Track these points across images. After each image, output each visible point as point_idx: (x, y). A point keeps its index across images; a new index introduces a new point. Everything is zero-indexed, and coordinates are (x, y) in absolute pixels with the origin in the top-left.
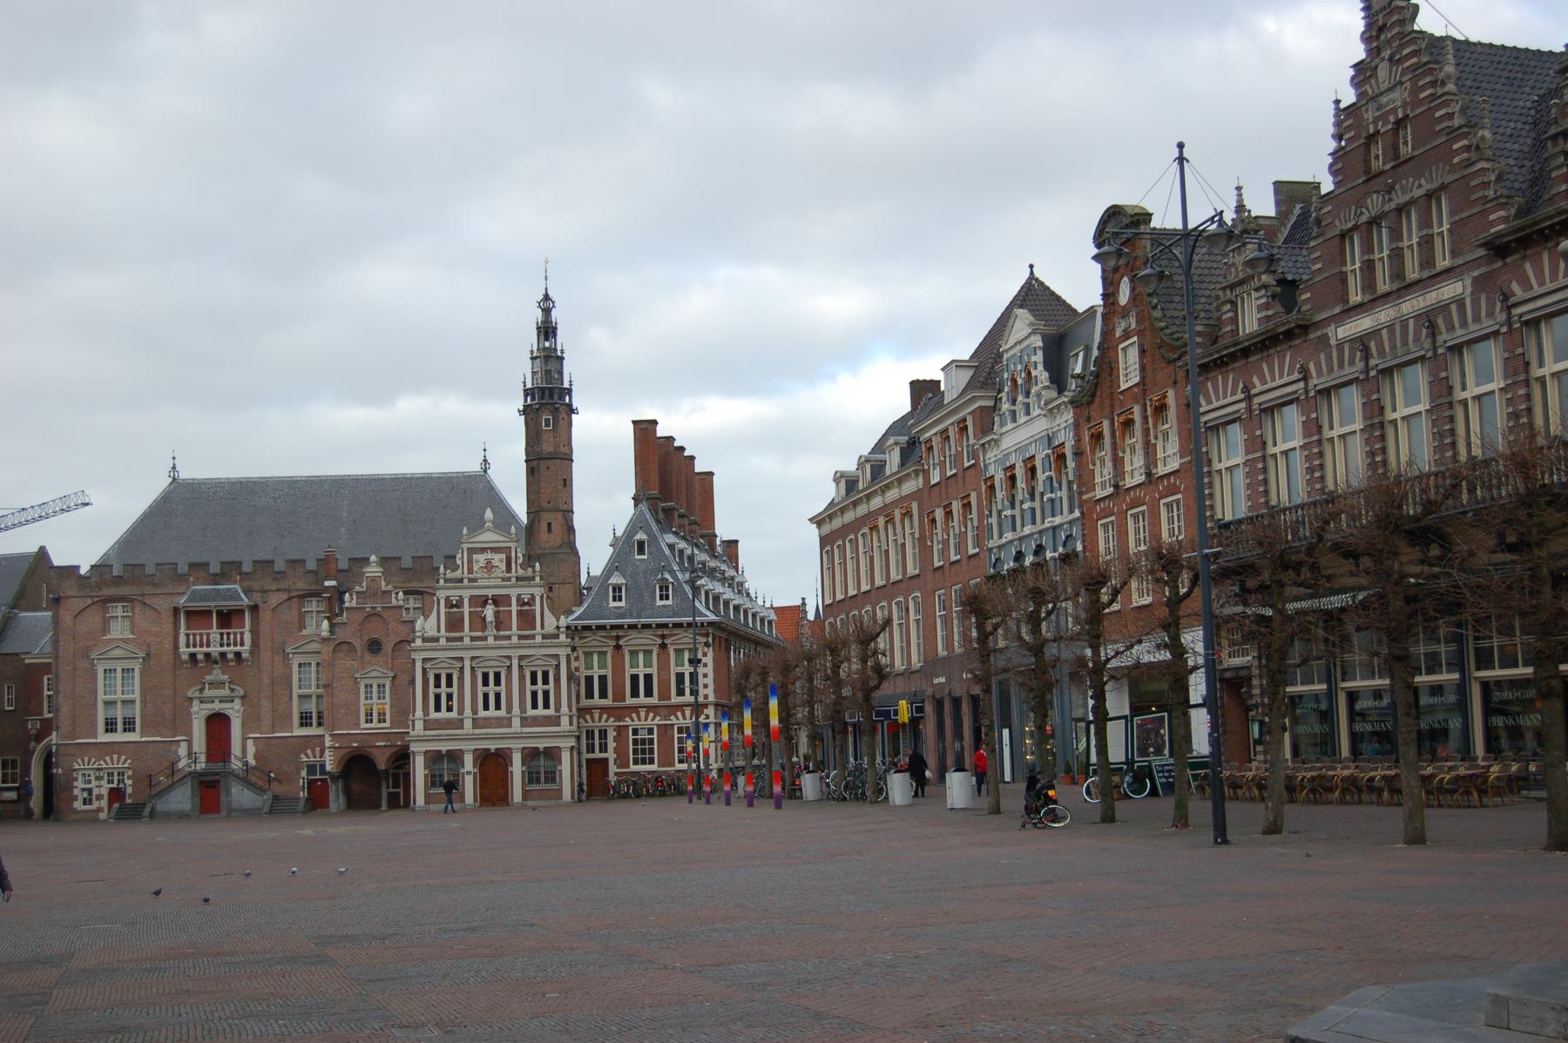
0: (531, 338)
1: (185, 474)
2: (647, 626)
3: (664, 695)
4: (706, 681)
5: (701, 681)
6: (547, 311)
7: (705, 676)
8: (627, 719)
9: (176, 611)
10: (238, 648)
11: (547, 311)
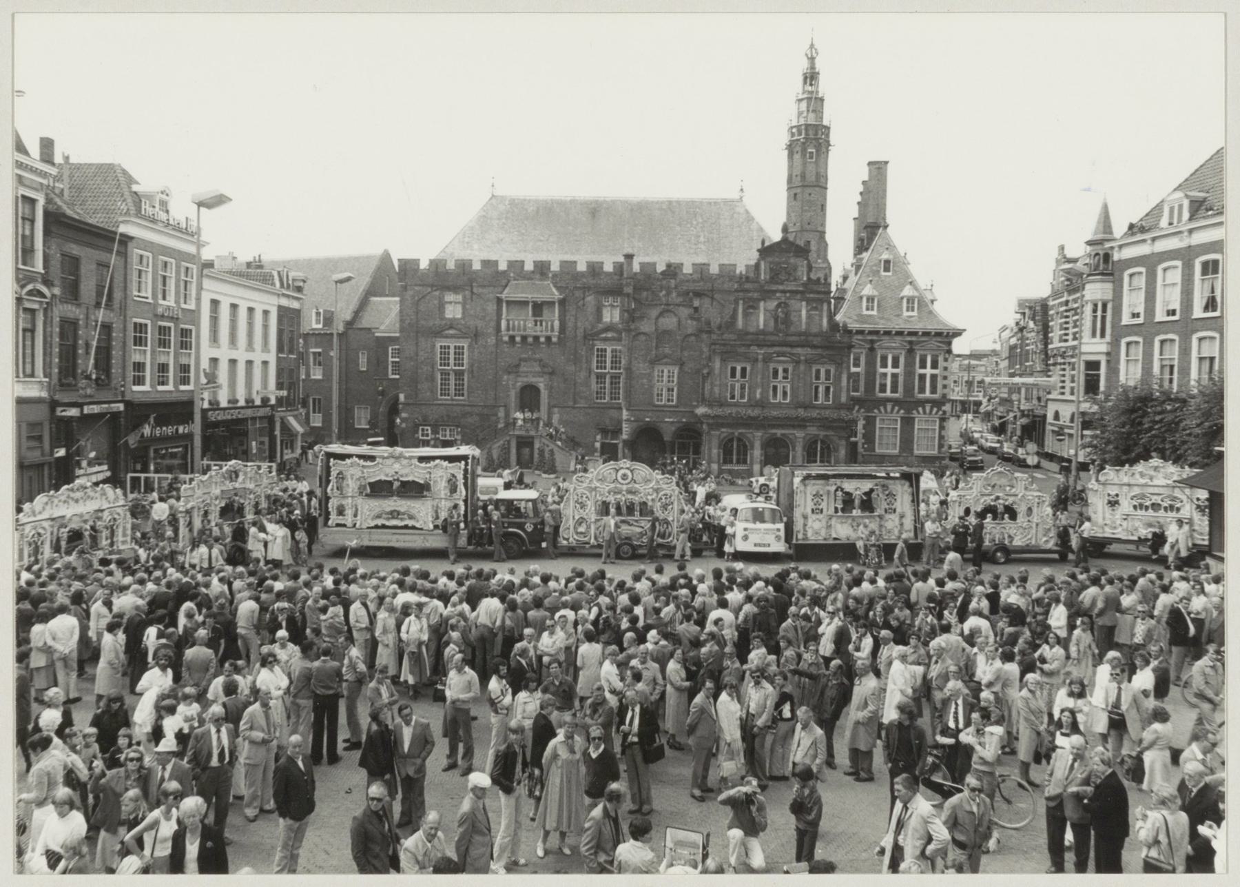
0: (796, 86)
1: (499, 192)
2: (900, 333)
6: (812, 60)
10: (549, 333)
11: (812, 60)
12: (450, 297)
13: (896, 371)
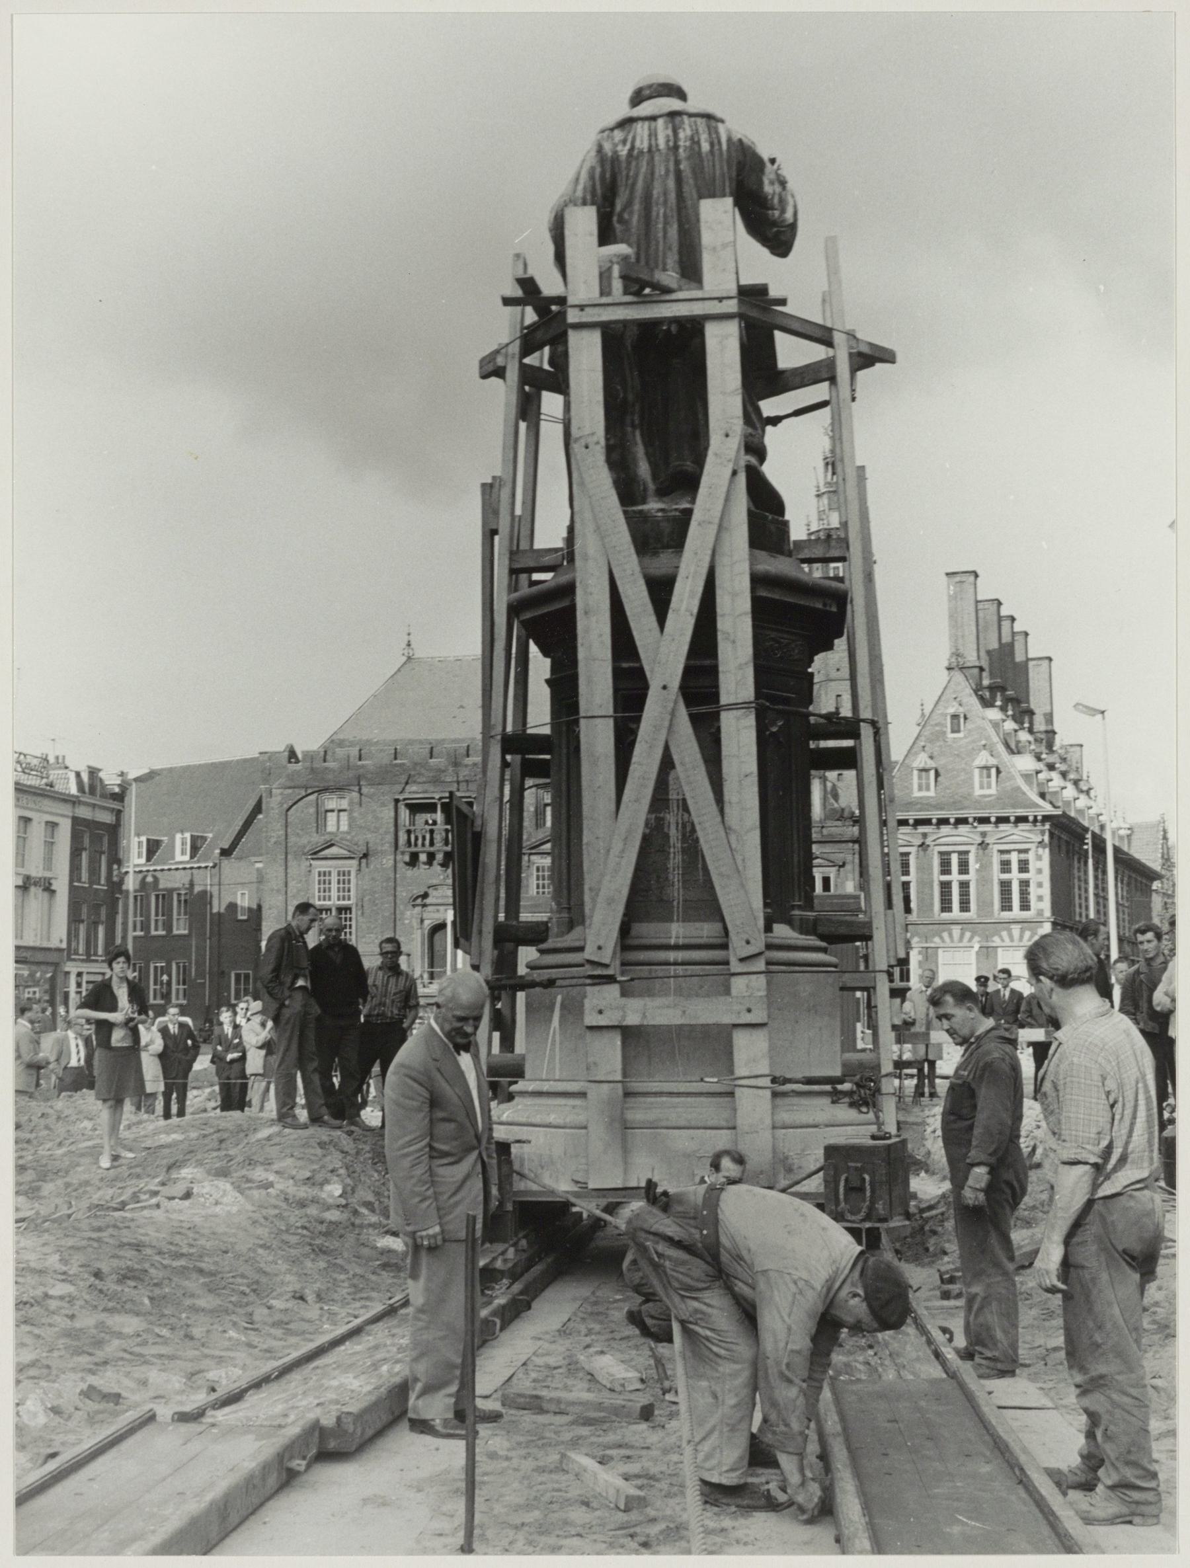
3: (985, 905)
4: (1041, 891)
5: (1033, 890)
7: (1040, 885)
8: (937, 939)
9: (397, 801)
12: (332, 802)
13: (964, 877)
